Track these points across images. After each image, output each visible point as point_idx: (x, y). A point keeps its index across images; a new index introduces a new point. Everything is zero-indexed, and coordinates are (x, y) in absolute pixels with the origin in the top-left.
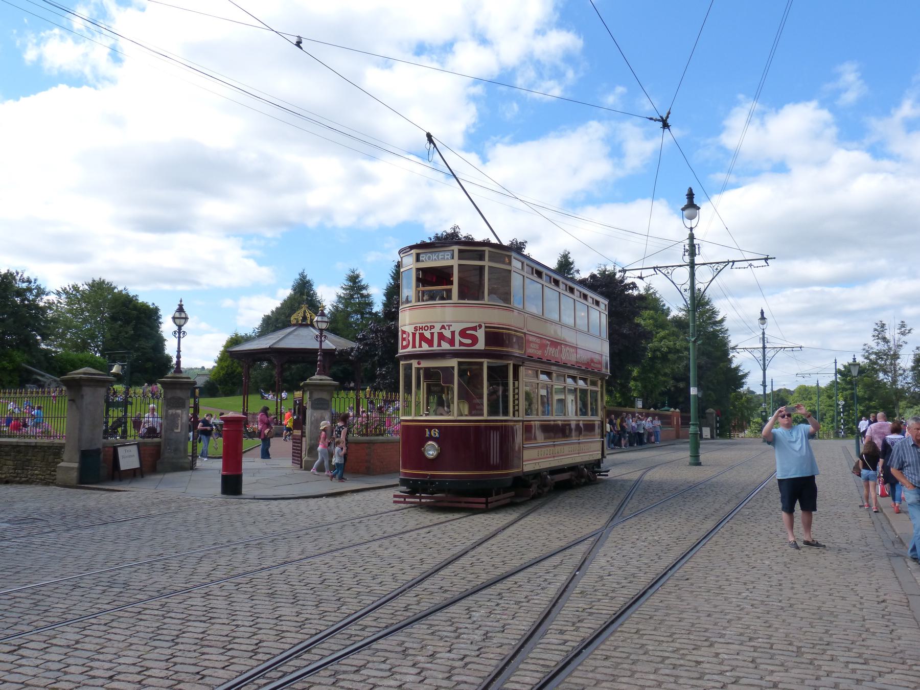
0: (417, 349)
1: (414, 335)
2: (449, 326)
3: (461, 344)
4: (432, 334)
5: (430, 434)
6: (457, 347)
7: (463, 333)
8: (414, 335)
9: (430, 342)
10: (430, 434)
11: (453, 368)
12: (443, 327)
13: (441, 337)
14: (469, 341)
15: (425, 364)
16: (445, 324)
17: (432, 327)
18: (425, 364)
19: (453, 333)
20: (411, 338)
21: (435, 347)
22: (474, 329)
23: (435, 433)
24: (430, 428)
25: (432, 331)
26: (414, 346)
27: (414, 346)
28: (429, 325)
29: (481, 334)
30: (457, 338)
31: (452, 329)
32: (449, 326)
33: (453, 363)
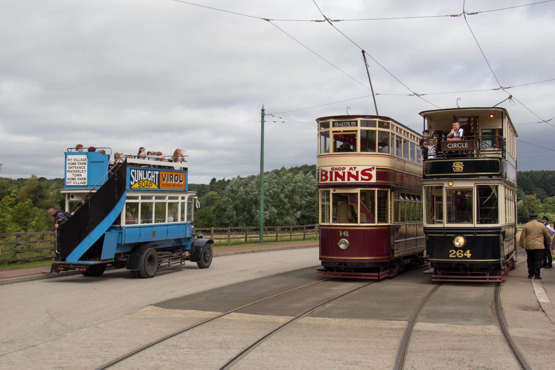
0: (334, 182)
1: (331, 173)
2: (355, 168)
3: (362, 179)
4: (344, 173)
5: (343, 234)
6: (360, 181)
7: (363, 173)
8: (331, 173)
9: (343, 178)
10: (343, 234)
11: (357, 194)
12: (351, 169)
13: (350, 175)
14: (367, 177)
15: (338, 191)
16: (352, 167)
17: (344, 169)
18: (338, 191)
19: (357, 172)
20: (329, 175)
21: (346, 181)
22: (370, 170)
23: (346, 234)
24: (343, 231)
25: (344, 171)
26: (331, 180)
27: (331, 180)
28: (342, 167)
29: (374, 173)
30: (360, 175)
31: (357, 170)
32: (355, 168)
33: (358, 191)
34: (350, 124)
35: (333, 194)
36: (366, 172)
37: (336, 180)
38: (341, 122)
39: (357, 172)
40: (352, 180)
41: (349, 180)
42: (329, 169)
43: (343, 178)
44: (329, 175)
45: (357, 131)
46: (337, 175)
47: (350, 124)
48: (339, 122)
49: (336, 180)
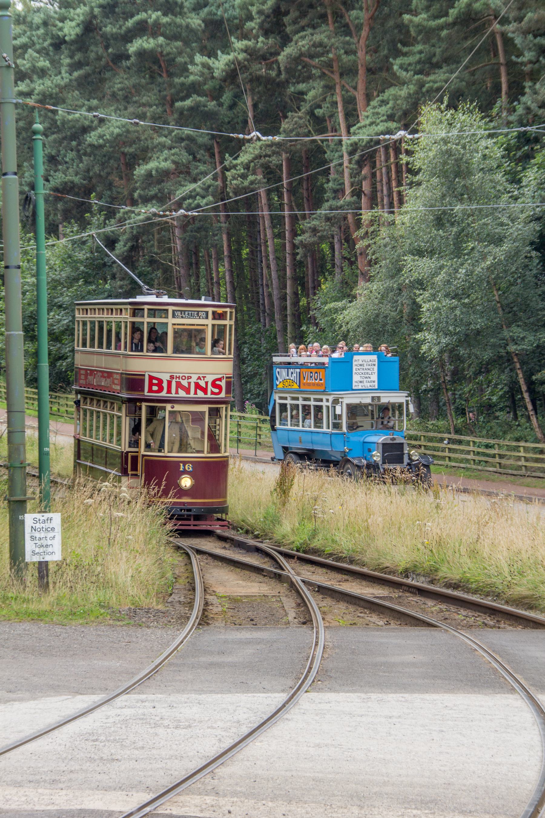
0: (173, 394)
1: (169, 383)
3: (213, 393)
4: (189, 384)
5: (184, 469)
6: (209, 395)
7: (214, 385)
8: (169, 383)
9: (188, 391)
10: (184, 469)
12: (199, 378)
13: (197, 386)
14: (216, 391)
19: (207, 383)
20: (165, 385)
21: (192, 395)
22: (220, 380)
23: (189, 468)
24: (185, 463)
26: (169, 391)
27: (169, 391)
29: (223, 384)
30: (210, 387)
31: (206, 380)
34: (198, 314)
35: (170, 412)
36: (217, 382)
37: (177, 393)
38: (185, 311)
39: (207, 383)
40: (200, 394)
41: (196, 393)
42: (165, 378)
43: (188, 391)
44: (165, 385)
45: (213, 326)
46: (179, 385)
47: (198, 314)
48: (181, 311)
49: (177, 393)
